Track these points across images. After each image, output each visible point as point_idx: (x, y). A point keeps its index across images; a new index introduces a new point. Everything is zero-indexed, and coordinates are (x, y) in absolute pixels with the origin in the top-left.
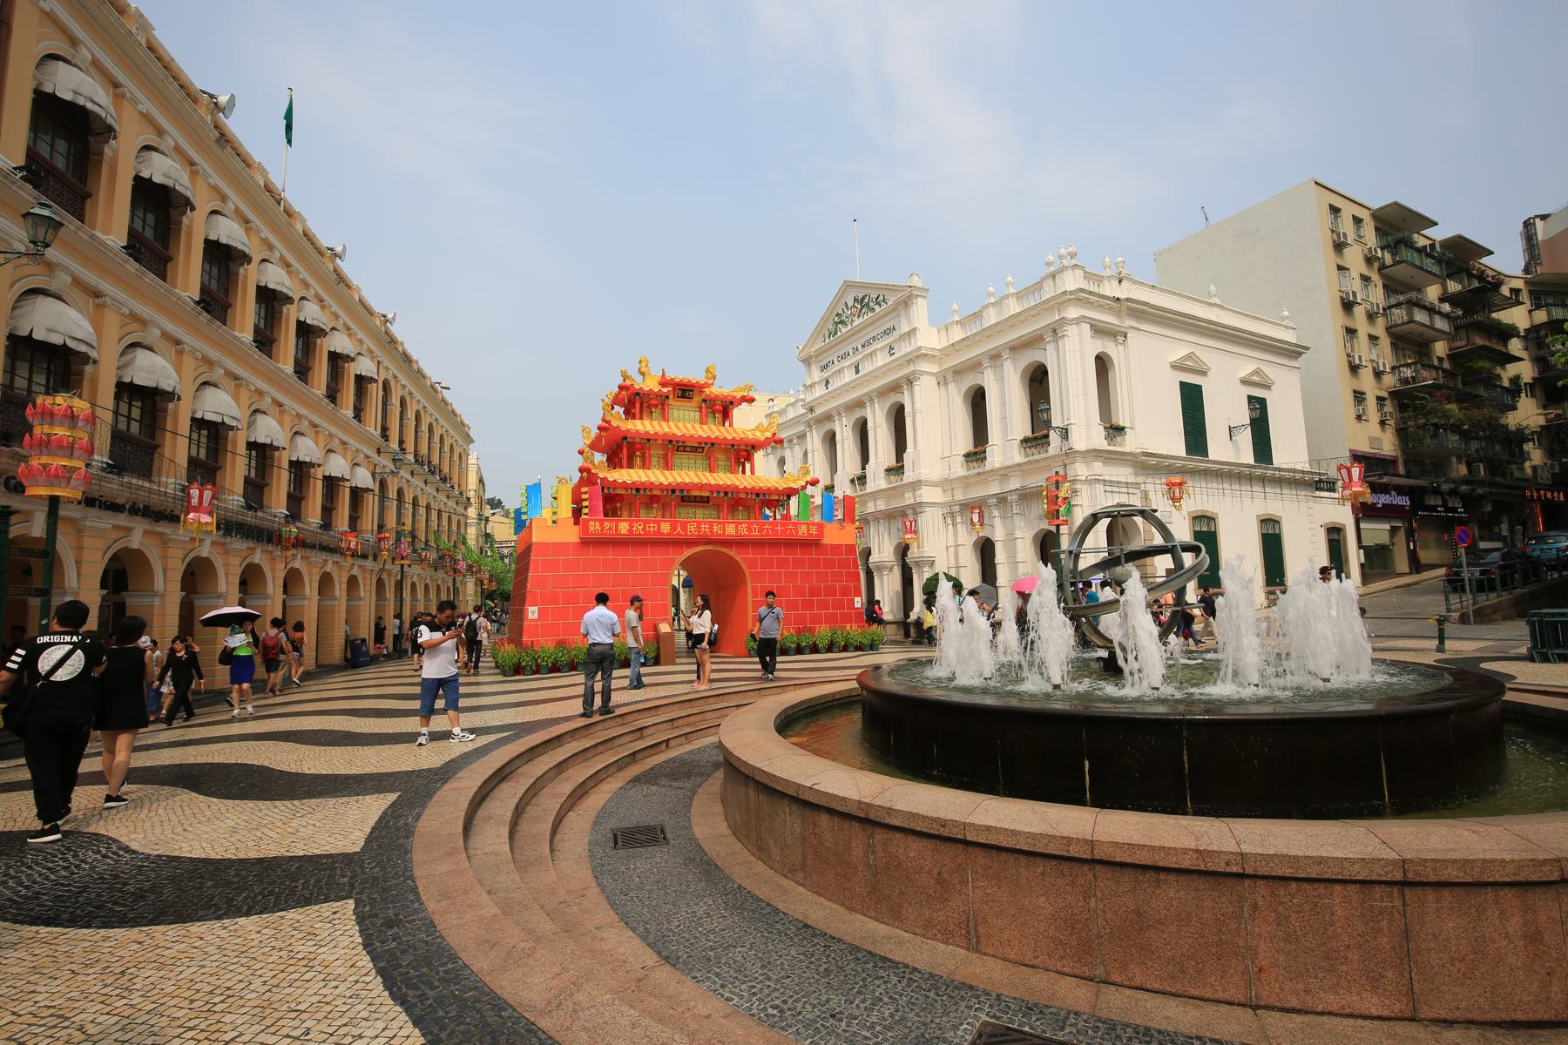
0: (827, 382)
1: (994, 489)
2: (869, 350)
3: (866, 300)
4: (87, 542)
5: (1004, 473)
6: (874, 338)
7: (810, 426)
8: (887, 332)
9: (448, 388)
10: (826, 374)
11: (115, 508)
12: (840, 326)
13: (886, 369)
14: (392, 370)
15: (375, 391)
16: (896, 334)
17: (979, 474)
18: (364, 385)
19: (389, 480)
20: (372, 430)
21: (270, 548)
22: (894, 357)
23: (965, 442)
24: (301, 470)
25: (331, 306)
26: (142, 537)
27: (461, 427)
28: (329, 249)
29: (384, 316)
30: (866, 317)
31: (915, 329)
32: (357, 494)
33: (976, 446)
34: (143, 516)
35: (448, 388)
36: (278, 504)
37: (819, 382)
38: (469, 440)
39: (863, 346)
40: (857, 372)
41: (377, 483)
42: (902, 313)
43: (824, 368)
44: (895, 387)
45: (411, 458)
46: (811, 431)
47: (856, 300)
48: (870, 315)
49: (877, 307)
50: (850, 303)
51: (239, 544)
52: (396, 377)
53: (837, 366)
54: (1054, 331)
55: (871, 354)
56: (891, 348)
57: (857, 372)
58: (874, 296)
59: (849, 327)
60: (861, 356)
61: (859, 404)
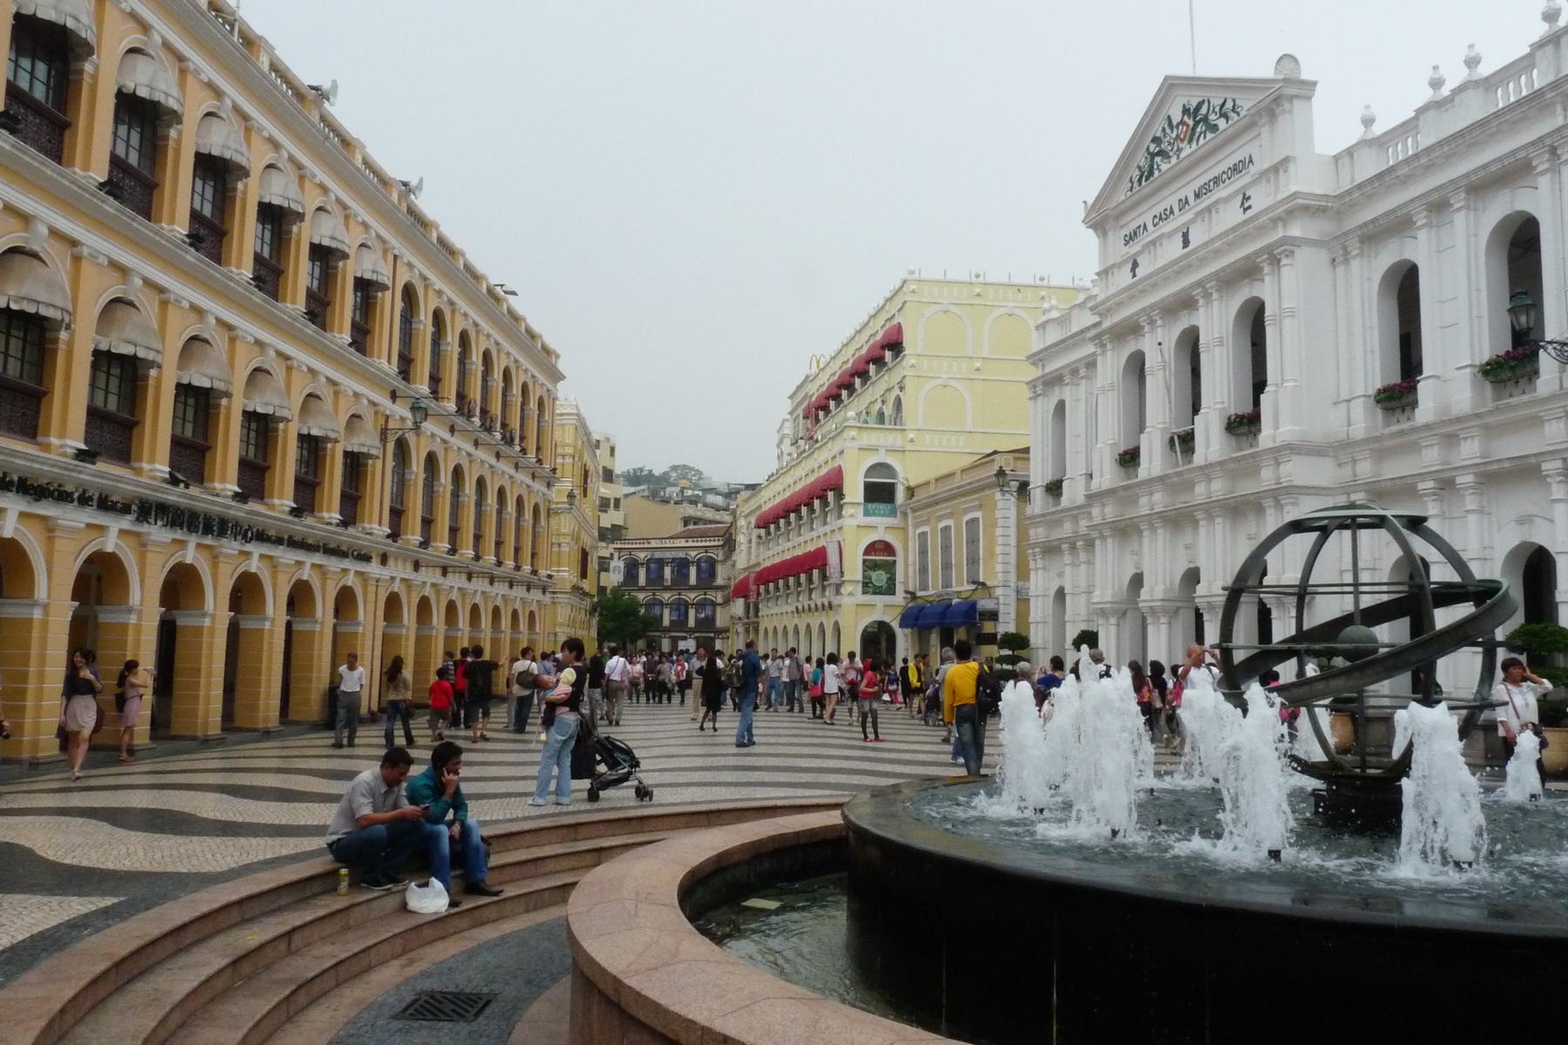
0: (1135, 265)
1: (1431, 457)
2: (1207, 201)
3: (1204, 110)
5: (1449, 431)
6: (1217, 180)
7: (1103, 346)
8: (1236, 169)
9: (514, 293)
10: (1135, 247)
12: (1158, 159)
13: (1237, 235)
14: (415, 267)
15: (390, 306)
16: (1253, 169)
17: (1402, 433)
18: (372, 294)
19: (411, 438)
20: (384, 361)
21: (209, 540)
22: (1250, 213)
23: (1377, 370)
24: (267, 430)
25: (314, 176)
26: (18, 521)
27: (545, 357)
28: (312, 88)
29: (405, 184)
30: (1202, 141)
31: (1286, 160)
32: (355, 464)
33: (1403, 378)
34: (17, 492)
35: (514, 293)
37: (1119, 265)
38: (557, 376)
39: (1197, 196)
40: (1186, 242)
41: (391, 446)
42: (1265, 131)
43: (1131, 238)
44: (1248, 271)
45: (451, 406)
46: (1104, 352)
47: (1186, 111)
48: (1209, 136)
49: (1222, 123)
50: (1176, 119)
51: (158, 533)
52: (425, 279)
53: (1153, 233)
54: (1553, 151)
55: (1208, 209)
56: (1246, 198)
57: (1186, 242)
58: (1217, 102)
59: (1174, 160)
60: (1189, 215)
61: (1186, 303)
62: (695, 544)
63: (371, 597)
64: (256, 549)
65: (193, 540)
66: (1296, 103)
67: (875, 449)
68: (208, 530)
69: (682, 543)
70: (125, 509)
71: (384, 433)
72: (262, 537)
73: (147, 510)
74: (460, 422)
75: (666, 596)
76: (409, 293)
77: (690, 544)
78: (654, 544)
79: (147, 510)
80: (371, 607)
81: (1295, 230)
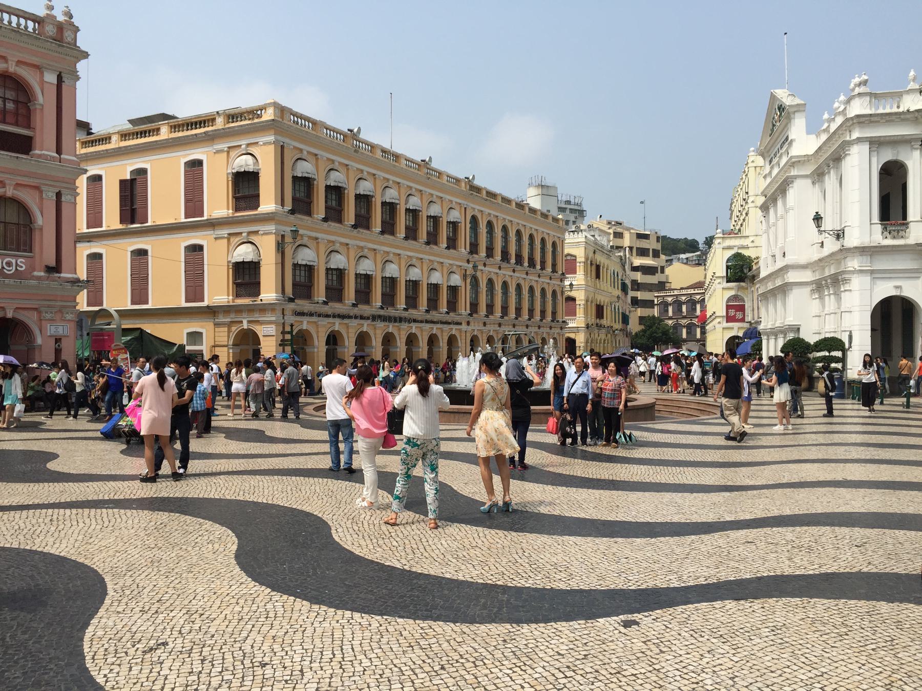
4: (320, 329)
11: (327, 316)
20: (463, 250)
21: (396, 324)
28: (422, 161)
36: (401, 303)
41: (468, 281)
62: (699, 292)
63: (463, 337)
64: (414, 325)
65: (391, 325)
66: (796, 114)
67: (729, 248)
68: (395, 321)
69: (692, 291)
70: (368, 318)
71: (465, 277)
72: (415, 321)
73: (374, 318)
74: (504, 265)
75: (684, 322)
76: (474, 220)
77: (696, 292)
78: (676, 293)
79: (374, 318)
80: (464, 341)
81: (794, 172)
